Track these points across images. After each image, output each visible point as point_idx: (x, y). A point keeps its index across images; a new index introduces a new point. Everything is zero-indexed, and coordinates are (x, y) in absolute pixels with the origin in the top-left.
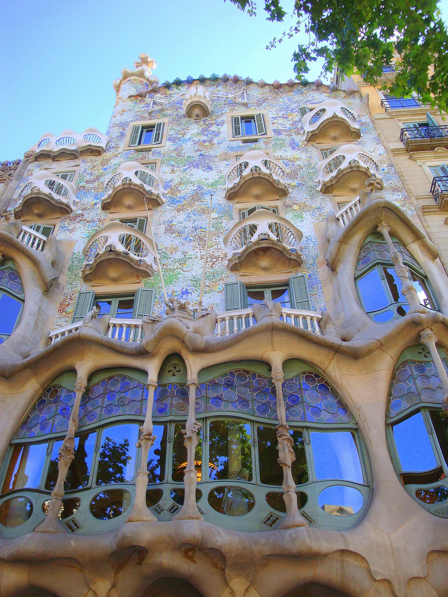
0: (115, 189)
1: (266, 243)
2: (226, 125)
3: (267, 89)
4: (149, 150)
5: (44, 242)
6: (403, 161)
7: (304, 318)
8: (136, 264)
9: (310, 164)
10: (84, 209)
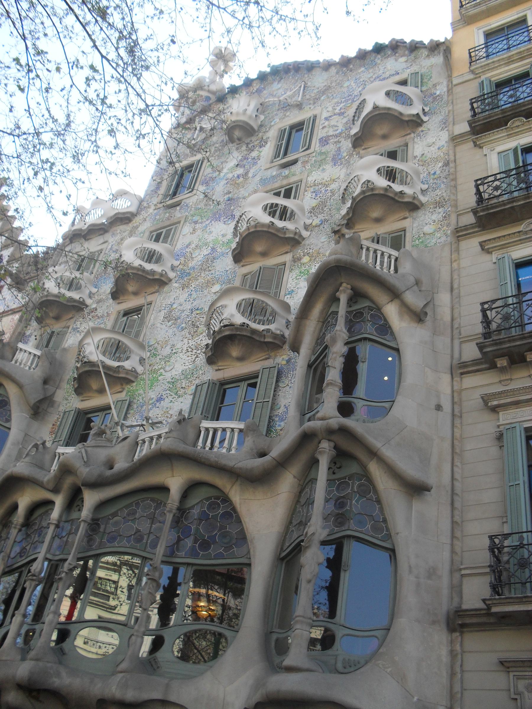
1: (229, 330)
2: (269, 144)
3: (333, 70)
4: (178, 204)
5: (39, 357)
8: (114, 372)
10: (99, 302)
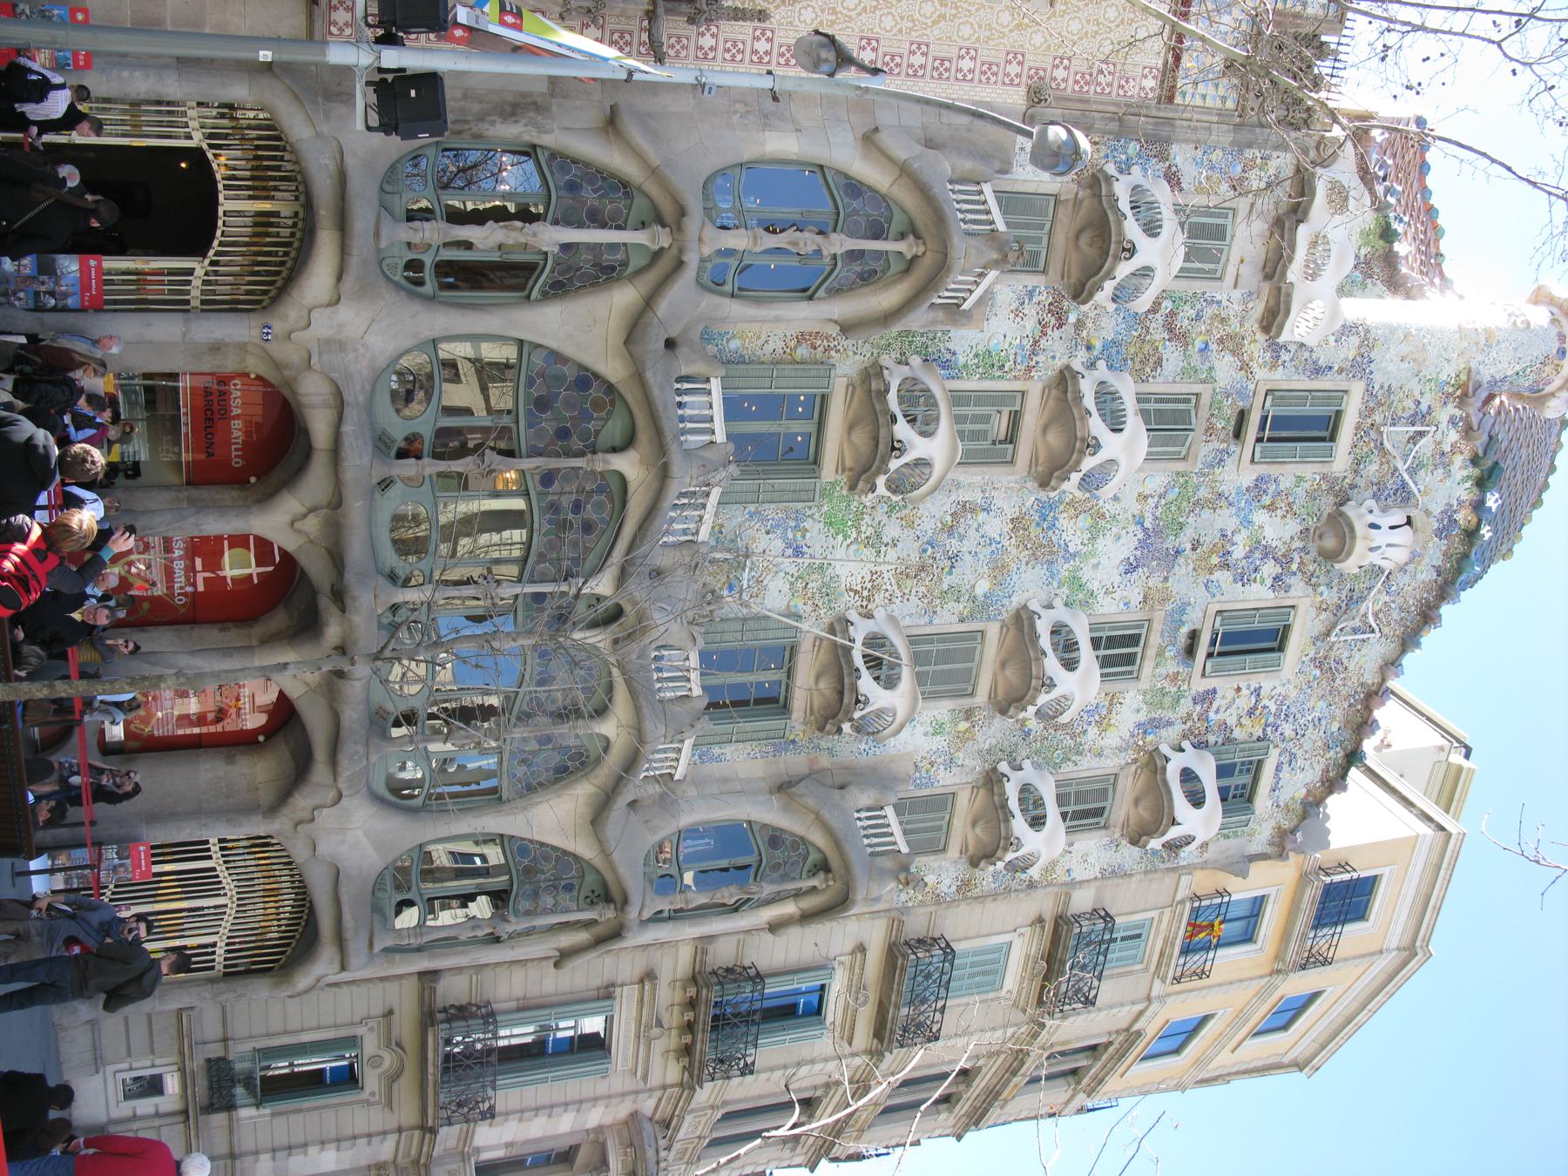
0: (1082, 419)
2: (1271, 594)
6: (1043, 903)
7: (677, 760)
9: (1079, 753)
